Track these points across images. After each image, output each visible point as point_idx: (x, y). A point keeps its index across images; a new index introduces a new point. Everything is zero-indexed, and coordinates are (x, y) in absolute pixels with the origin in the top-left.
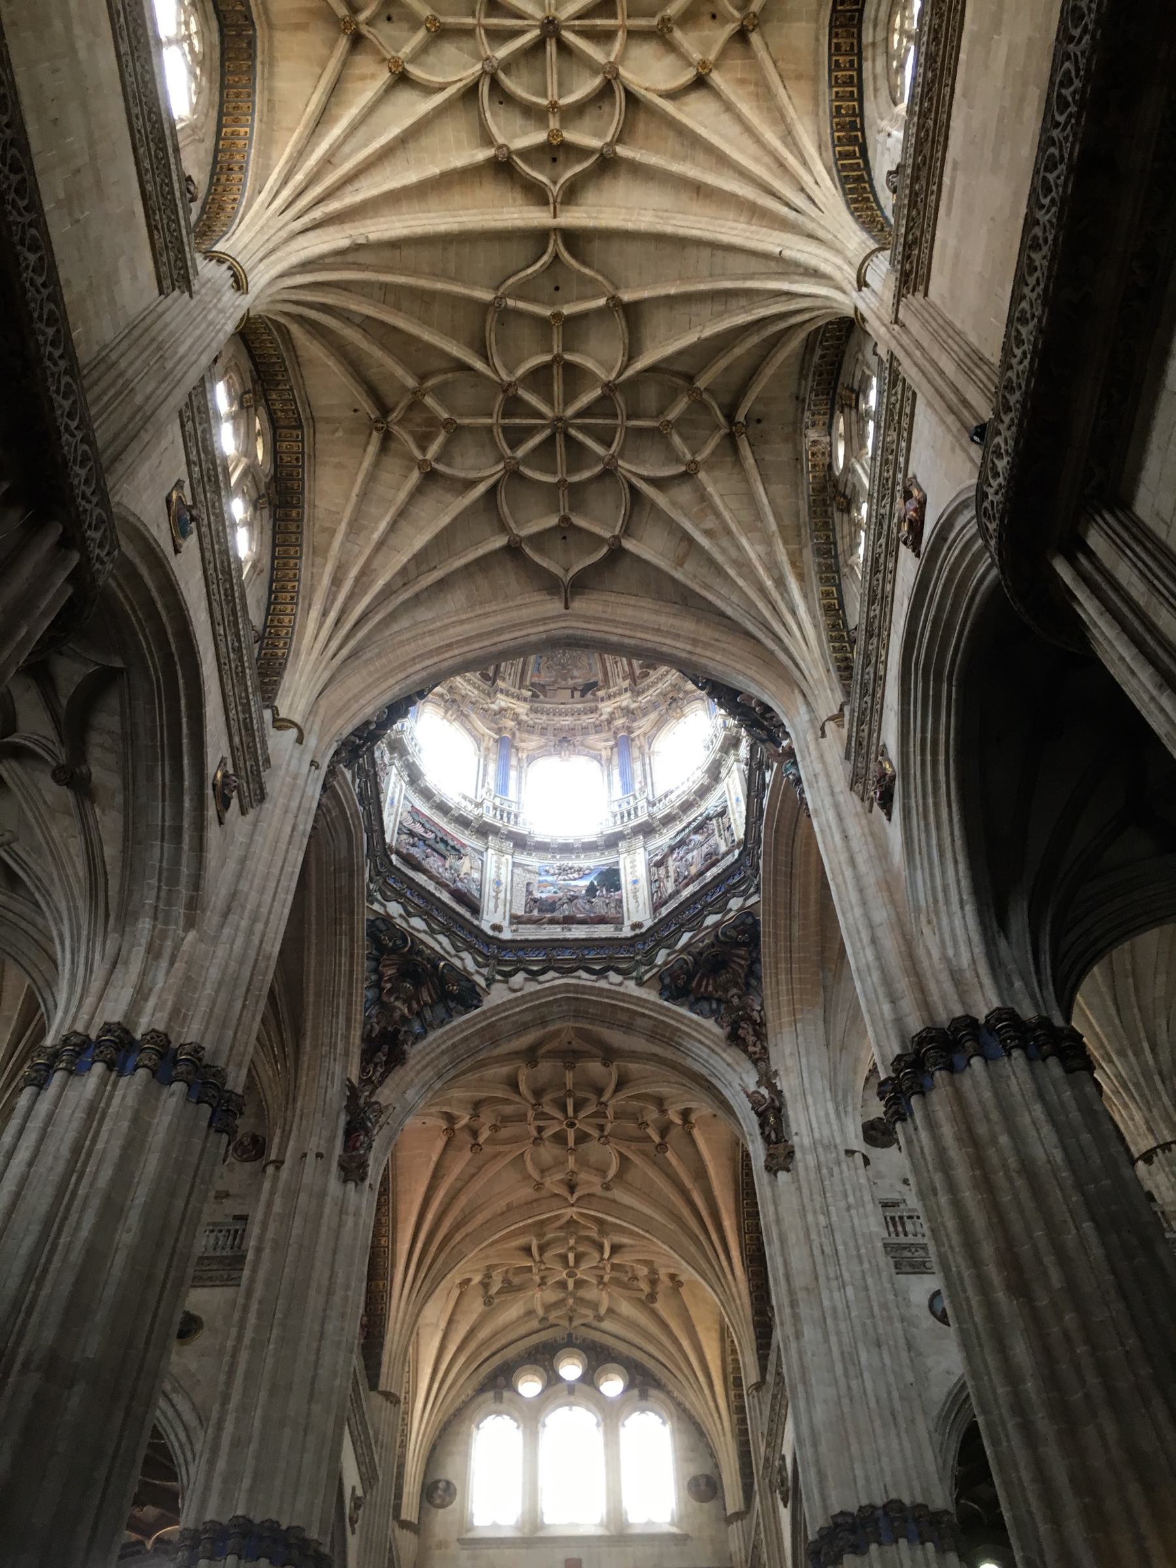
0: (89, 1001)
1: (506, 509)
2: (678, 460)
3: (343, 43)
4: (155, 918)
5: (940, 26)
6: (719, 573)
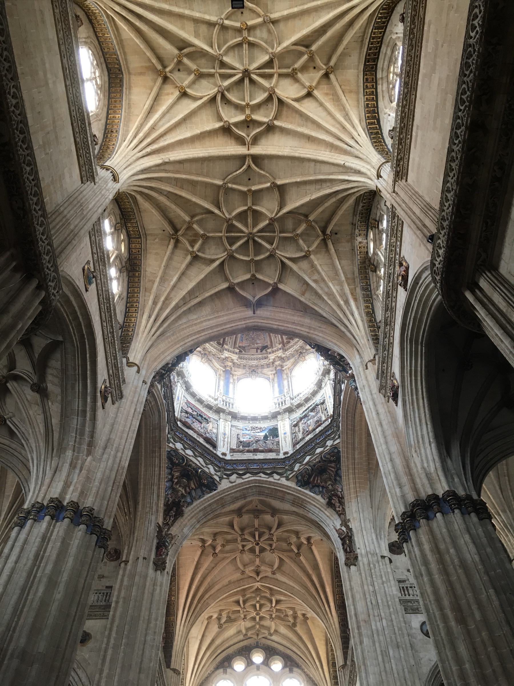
0: (44, 488)
1: (228, 272)
2: (302, 250)
3: (160, 80)
4: (74, 451)
5: (410, 70)
6: (320, 298)
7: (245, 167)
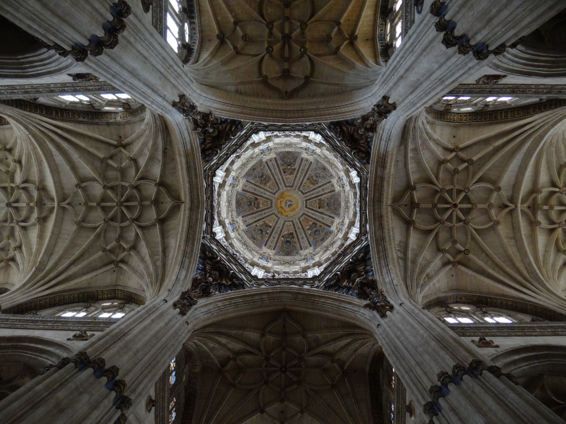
3: (11, 263)
7: (67, 207)
